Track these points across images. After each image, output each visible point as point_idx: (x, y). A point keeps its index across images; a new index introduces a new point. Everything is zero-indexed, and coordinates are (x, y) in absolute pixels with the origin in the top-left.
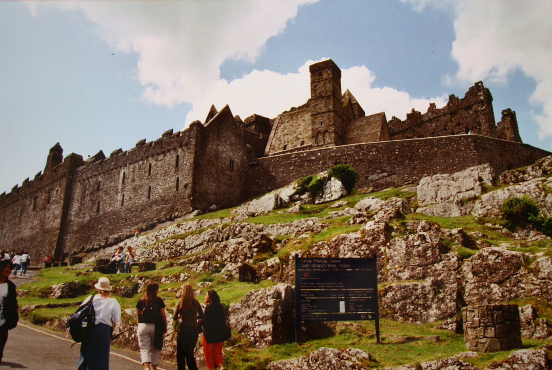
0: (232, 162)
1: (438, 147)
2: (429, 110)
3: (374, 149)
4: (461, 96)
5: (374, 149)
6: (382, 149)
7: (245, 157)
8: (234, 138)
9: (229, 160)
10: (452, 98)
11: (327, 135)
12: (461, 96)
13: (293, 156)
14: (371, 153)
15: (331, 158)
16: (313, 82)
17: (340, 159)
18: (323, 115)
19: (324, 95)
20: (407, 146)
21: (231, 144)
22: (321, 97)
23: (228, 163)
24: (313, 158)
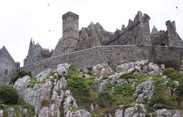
0: (6, 71)
1: (84, 54)
2: (122, 28)
3: (59, 59)
4: (133, 20)
5: (59, 59)
6: (62, 58)
7: (14, 68)
8: (7, 60)
9: (5, 70)
10: (130, 21)
11: (68, 49)
12: (133, 20)
13: (31, 65)
14: (58, 61)
15: (43, 64)
16: (63, 24)
17: (46, 65)
18: (67, 39)
19: (67, 30)
20: (72, 56)
21: (6, 63)
22: (66, 31)
23: (4, 71)
24: (37, 65)
